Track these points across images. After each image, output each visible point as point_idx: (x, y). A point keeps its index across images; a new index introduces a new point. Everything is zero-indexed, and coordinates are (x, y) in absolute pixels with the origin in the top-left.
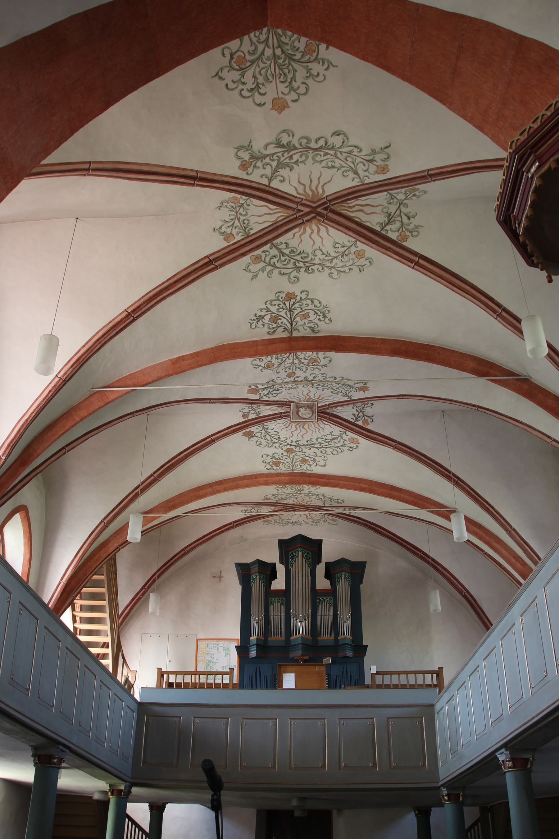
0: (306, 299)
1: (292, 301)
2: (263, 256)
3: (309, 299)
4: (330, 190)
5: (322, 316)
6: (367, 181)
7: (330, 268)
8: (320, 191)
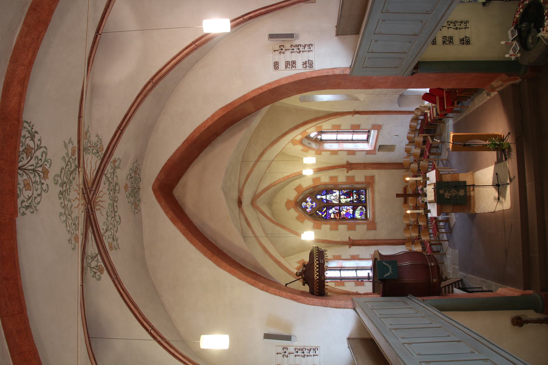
0: (42, 188)
1: (42, 174)
2: (73, 157)
3: (41, 192)
4: (98, 213)
5: (27, 204)
6: (104, 238)
7: (65, 214)
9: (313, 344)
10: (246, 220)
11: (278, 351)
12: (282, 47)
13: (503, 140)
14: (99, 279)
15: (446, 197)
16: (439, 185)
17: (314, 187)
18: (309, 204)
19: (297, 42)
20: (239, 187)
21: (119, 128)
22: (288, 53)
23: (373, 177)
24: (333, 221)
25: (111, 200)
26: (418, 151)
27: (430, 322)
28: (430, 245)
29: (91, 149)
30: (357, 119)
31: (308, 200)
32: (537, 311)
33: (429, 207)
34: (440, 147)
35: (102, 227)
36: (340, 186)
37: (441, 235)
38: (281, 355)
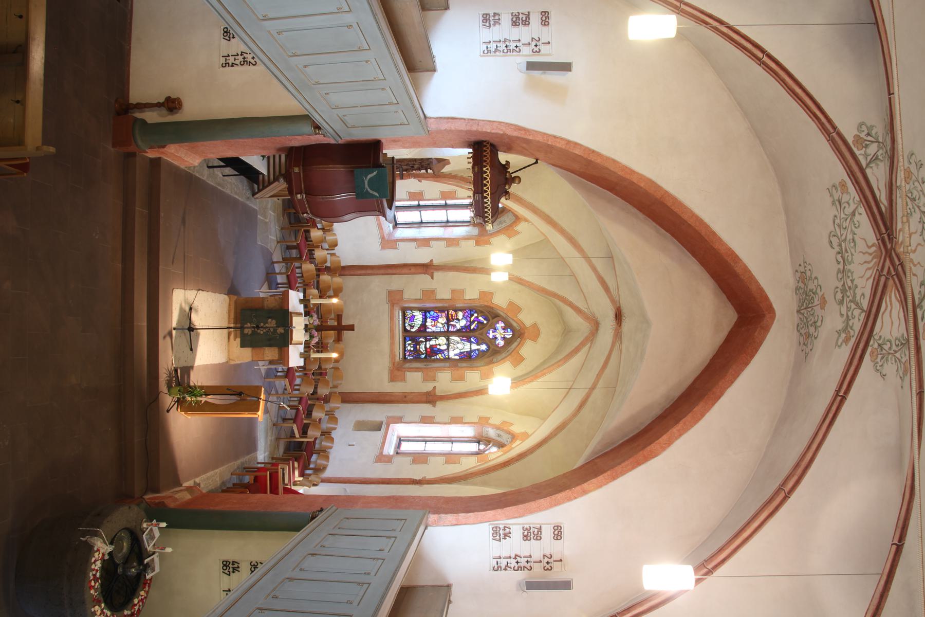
4: (872, 238)
6: (857, 198)
8: (874, 249)
9: (491, 60)
10: (606, 289)
11: (547, 47)
12: (548, 566)
13: (178, 401)
14: (861, 125)
15: (274, 321)
16: (283, 341)
17: (492, 362)
18: (500, 334)
19: (521, 575)
20: (621, 343)
21: (844, 398)
22: (537, 556)
23: (393, 379)
24: (459, 305)
25: (849, 271)
26: (317, 414)
27: (309, 70)
28: (301, 257)
29: (894, 347)
30: (417, 472)
31: (501, 343)
32: (143, 122)
33: (301, 308)
34: (280, 420)
35: (863, 218)
36: (447, 364)
37: (284, 271)
38: (542, 41)
